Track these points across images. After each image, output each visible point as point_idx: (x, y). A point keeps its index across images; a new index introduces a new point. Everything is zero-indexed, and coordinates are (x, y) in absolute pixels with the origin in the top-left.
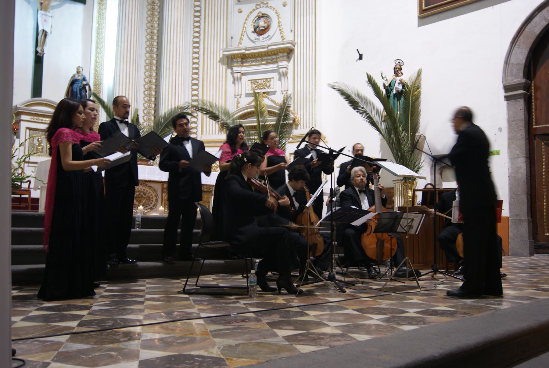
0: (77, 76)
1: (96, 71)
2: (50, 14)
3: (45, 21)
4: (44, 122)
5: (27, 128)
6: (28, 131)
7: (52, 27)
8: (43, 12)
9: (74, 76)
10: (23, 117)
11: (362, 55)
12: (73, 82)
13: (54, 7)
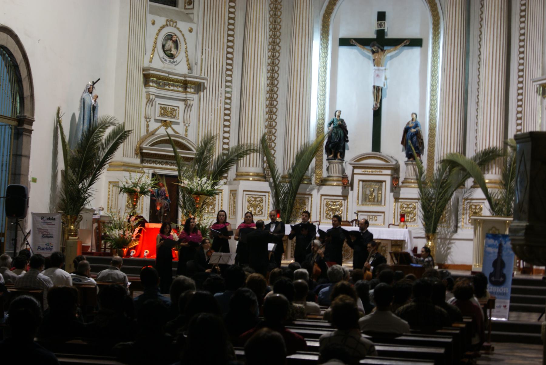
0: (411, 123)
1: (431, 114)
2: (383, 68)
3: (378, 76)
4: (374, 173)
5: (360, 180)
7: (386, 79)
8: (376, 68)
9: (408, 123)
12: (407, 130)
13: (392, 57)
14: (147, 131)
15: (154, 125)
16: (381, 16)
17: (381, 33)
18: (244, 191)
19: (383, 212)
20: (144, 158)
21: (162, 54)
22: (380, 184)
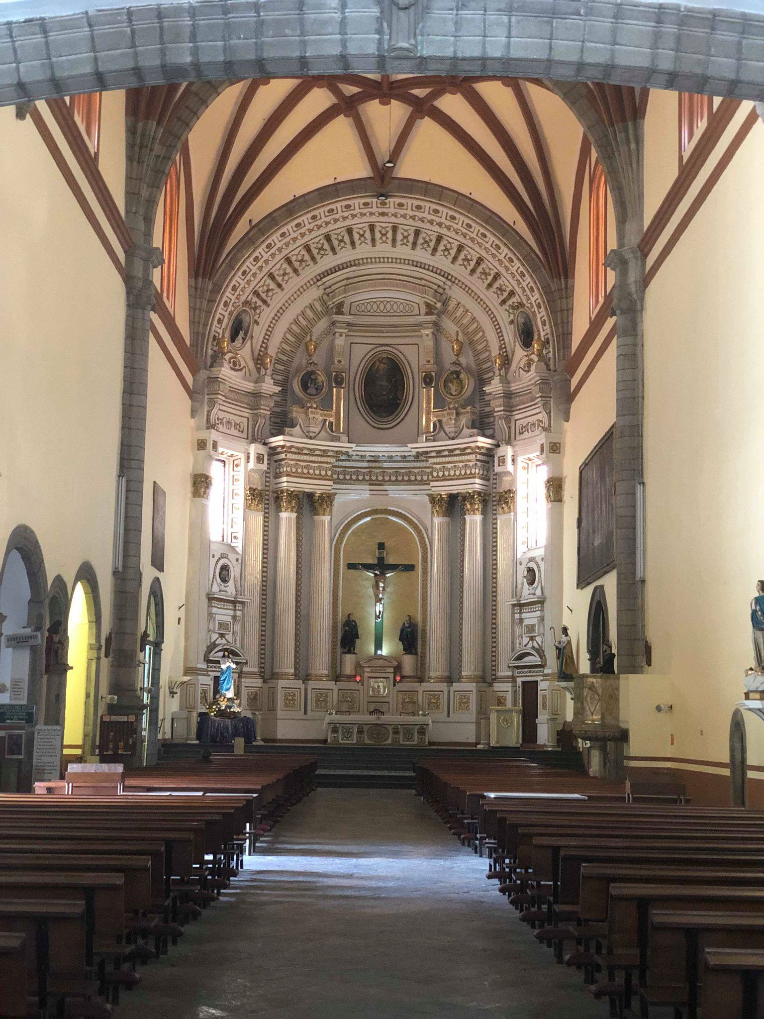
16: (381, 546)
17: (381, 559)
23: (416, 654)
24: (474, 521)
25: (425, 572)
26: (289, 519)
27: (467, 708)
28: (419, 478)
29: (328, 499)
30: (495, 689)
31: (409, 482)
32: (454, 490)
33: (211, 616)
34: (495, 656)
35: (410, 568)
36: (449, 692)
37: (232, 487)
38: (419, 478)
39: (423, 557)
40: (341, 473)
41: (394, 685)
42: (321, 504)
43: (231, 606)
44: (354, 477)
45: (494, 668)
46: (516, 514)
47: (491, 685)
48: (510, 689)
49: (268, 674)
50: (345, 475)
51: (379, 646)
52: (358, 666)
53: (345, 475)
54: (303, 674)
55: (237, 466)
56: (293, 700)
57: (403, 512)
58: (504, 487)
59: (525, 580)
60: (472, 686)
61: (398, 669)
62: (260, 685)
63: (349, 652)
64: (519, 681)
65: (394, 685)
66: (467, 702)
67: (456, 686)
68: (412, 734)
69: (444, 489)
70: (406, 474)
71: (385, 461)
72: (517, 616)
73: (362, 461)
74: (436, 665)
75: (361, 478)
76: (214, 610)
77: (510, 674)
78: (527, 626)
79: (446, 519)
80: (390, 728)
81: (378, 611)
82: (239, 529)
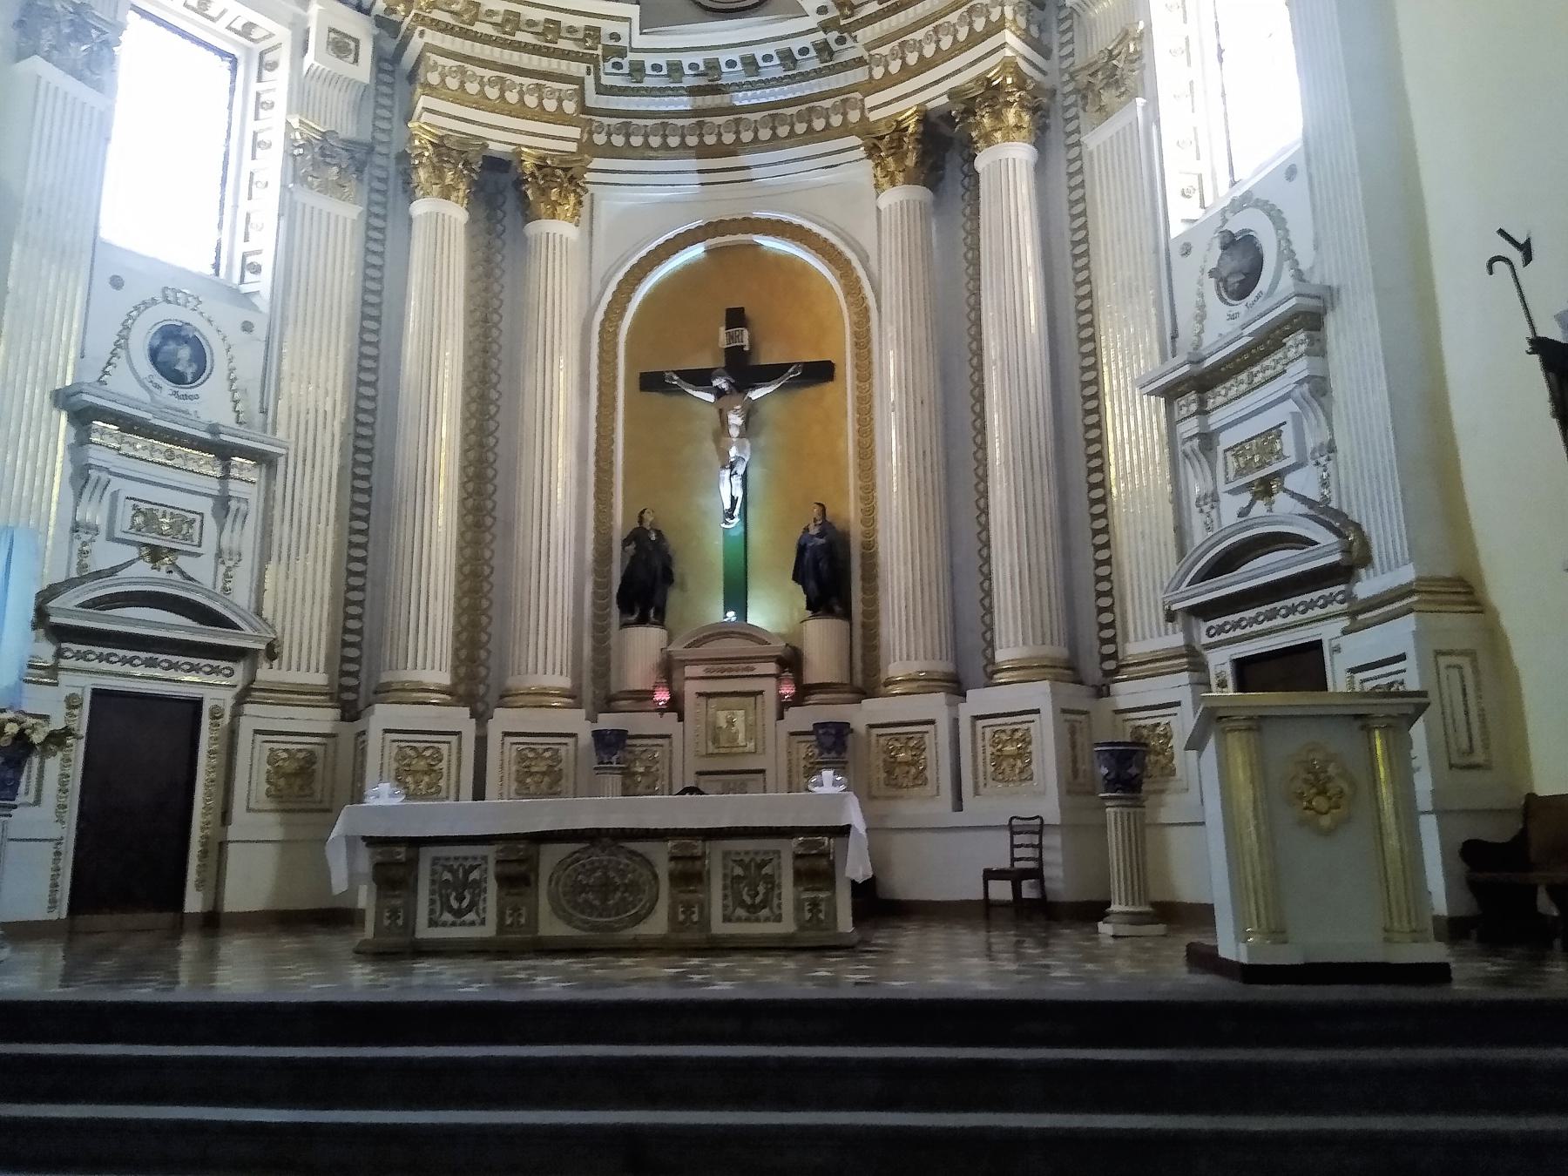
6: (702, 700)
10: (690, 671)
11: (1528, 242)
14: (82, 567)
15: (105, 555)
18: (387, 731)
19: (762, 771)
20: (64, 645)
21: (146, 368)
22: (752, 699)
23: (847, 615)
24: (1007, 162)
25: (865, 373)
26: (437, 219)
27: (1025, 775)
28: (836, 120)
29: (563, 177)
30: (1123, 703)
31: (811, 136)
32: (937, 98)
33: (81, 476)
34: (1107, 592)
35: (821, 372)
36: (955, 722)
37: (252, 125)
38: (836, 120)
39: (855, 334)
40: (618, 130)
41: (781, 717)
42: (544, 192)
43: (207, 464)
44: (655, 141)
45: (1110, 632)
46: (1153, 101)
47: (1102, 691)
48: (1185, 695)
49: (350, 694)
50: (628, 136)
51: (737, 596)
52: (668, 669)
53: (628, 136)
54: (477, 686)
55: (274, 66)
56: (430, 770)
57: (797, 221)
58: (1103, 39)
59: (1211, 283)
60: (1038, 694)
61: (791, 662)
62: (326, 728)
63: (643, 621)
64: (1220, 661)
65: (781, 717)
66: (1020, 755)
67: (980, 700)
68: (772, 883)
69: (901, 104)
70: (800, 117)
71: (740, 87)
72: (1190, 427)
73: (675, 92)
74: (906, 645)
75: (674, 141)
76: (95, 455)
77: (1177, 640)
78: (1237, 450)
79: (919, 193)
80: (660, 854)
81: (729, 499)
82: (265, 243)
